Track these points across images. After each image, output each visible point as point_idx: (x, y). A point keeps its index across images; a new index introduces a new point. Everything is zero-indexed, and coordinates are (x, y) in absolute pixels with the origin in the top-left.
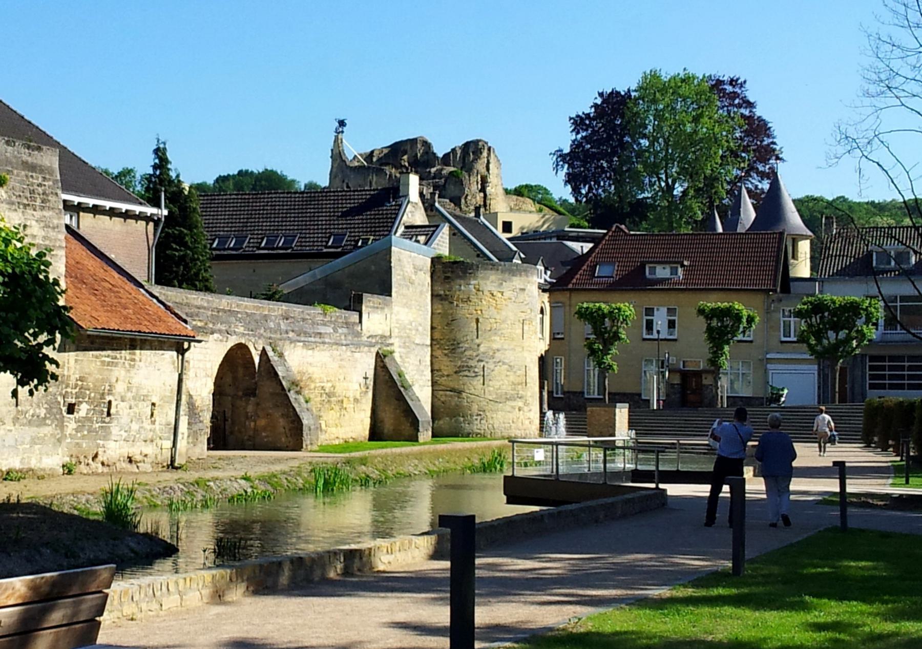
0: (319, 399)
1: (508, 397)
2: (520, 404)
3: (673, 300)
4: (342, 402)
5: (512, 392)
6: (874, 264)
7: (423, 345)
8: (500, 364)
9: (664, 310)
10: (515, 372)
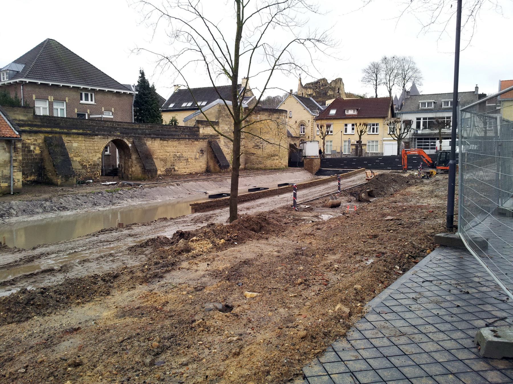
0: (173, 159)
2: (277, 158)
3: (354, 121)
6: (420, 107)
9: (351, 125)
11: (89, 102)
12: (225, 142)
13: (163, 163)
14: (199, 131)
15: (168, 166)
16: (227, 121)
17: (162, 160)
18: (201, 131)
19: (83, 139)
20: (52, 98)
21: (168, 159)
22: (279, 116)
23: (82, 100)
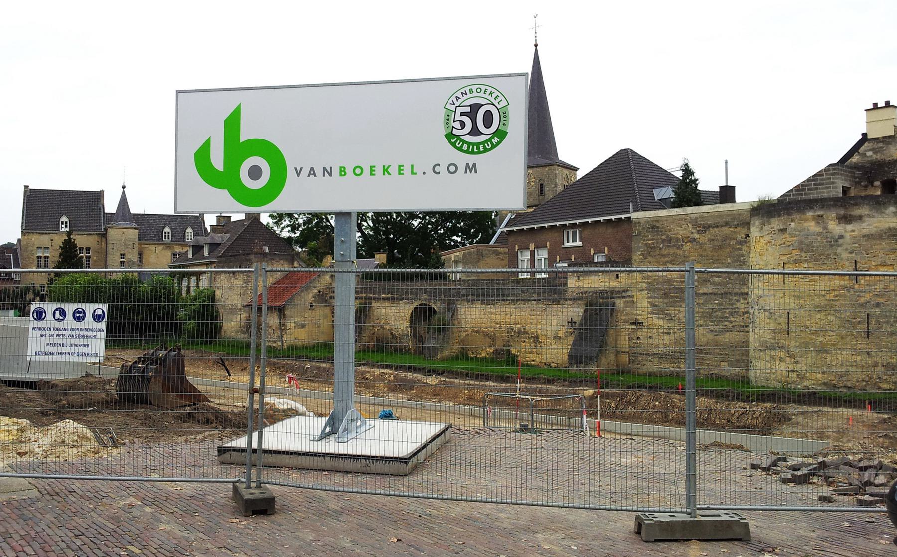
1: (768, 345)
2: (782, 354)
4: (537, 337)
5: (773, 341)
7: (726, 294)
8: (762, 311)
10: (776, 319)
11: (578, 243)
12: (653, 305)
13: (489, 340)
14: (566, 285)
15: (499, 346)
16: (664, 256)
17: (487, 335)
18: (572, 283)
19: (389, 305)
20: (533, 246)
21: (497, 335)
22: (785, 224)
23: (568, 241)
